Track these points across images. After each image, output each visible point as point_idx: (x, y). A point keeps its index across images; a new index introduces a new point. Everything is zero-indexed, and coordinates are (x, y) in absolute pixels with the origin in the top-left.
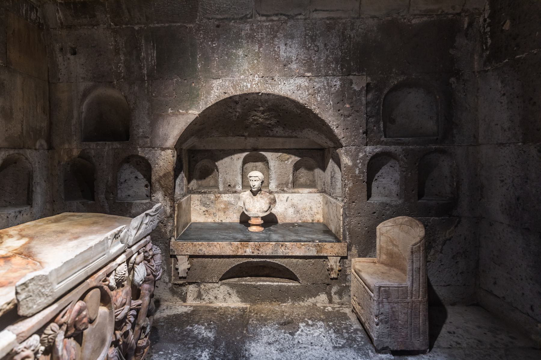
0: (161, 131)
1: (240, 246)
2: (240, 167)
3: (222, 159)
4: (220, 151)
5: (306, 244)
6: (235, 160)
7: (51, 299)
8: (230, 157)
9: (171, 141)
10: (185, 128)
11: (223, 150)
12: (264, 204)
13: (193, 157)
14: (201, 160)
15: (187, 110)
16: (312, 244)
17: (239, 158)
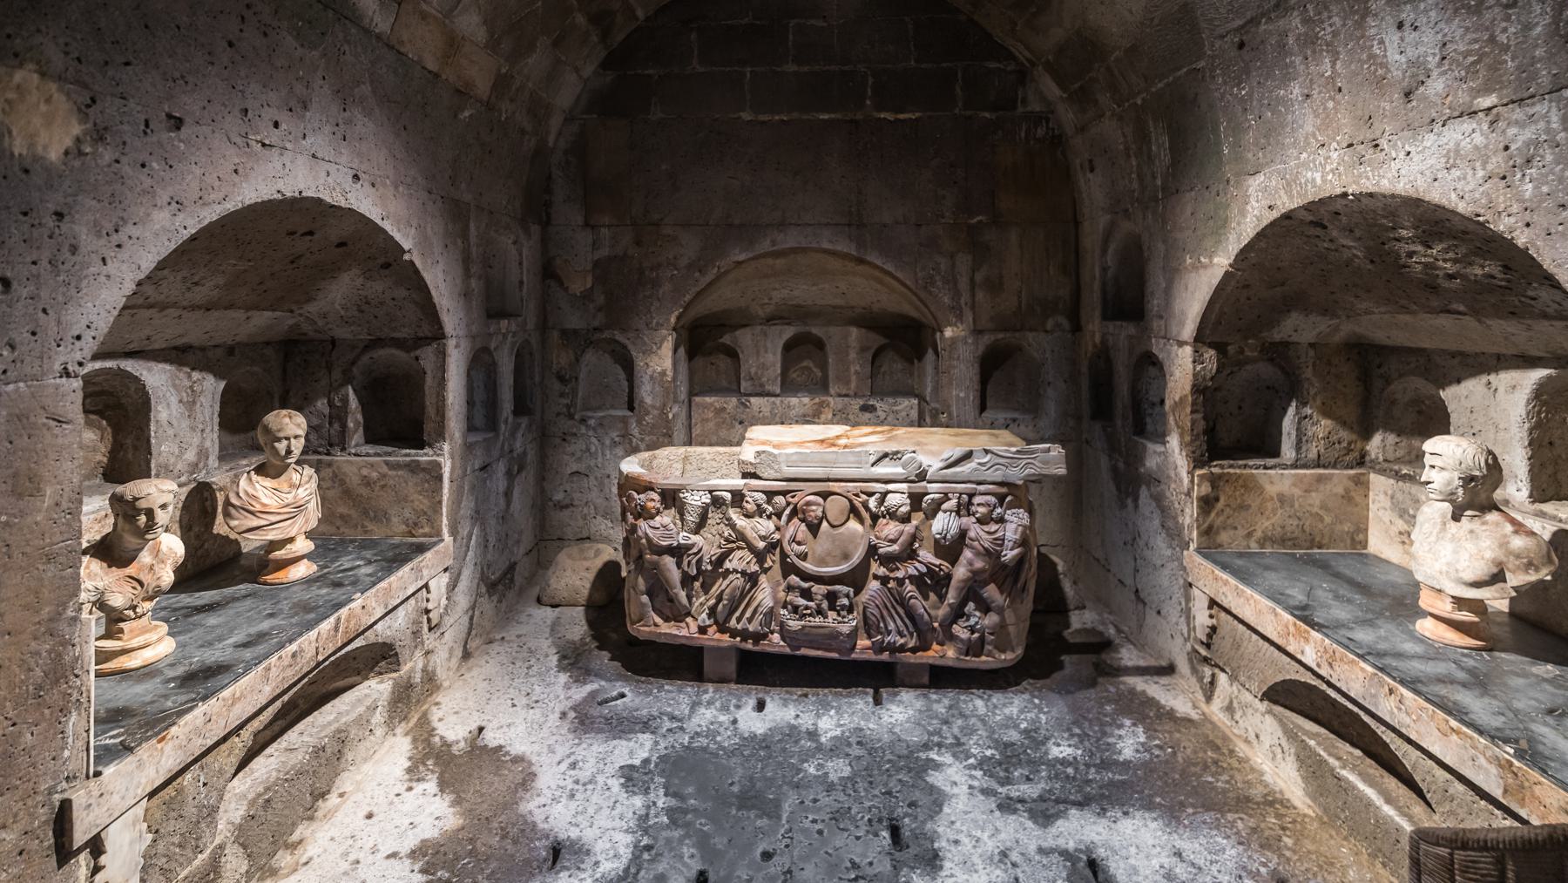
0: (1177, 306)
1: (1292, 629)
2: (1519, 419)
3: (1459, 381)
4: (1453, 355)
5: (1465, 733)
6: (1501, 390)
7: (778, 476)
8: (1484, 379)
9: (1188, 330)
10: (1208, 298)
11: (1461, 354)
12: (1467, 556)
13: (1379, 366)
14: (1401, 376)
15: (1211, 257)
16: (1486, 747)
17: (1514, 387)
